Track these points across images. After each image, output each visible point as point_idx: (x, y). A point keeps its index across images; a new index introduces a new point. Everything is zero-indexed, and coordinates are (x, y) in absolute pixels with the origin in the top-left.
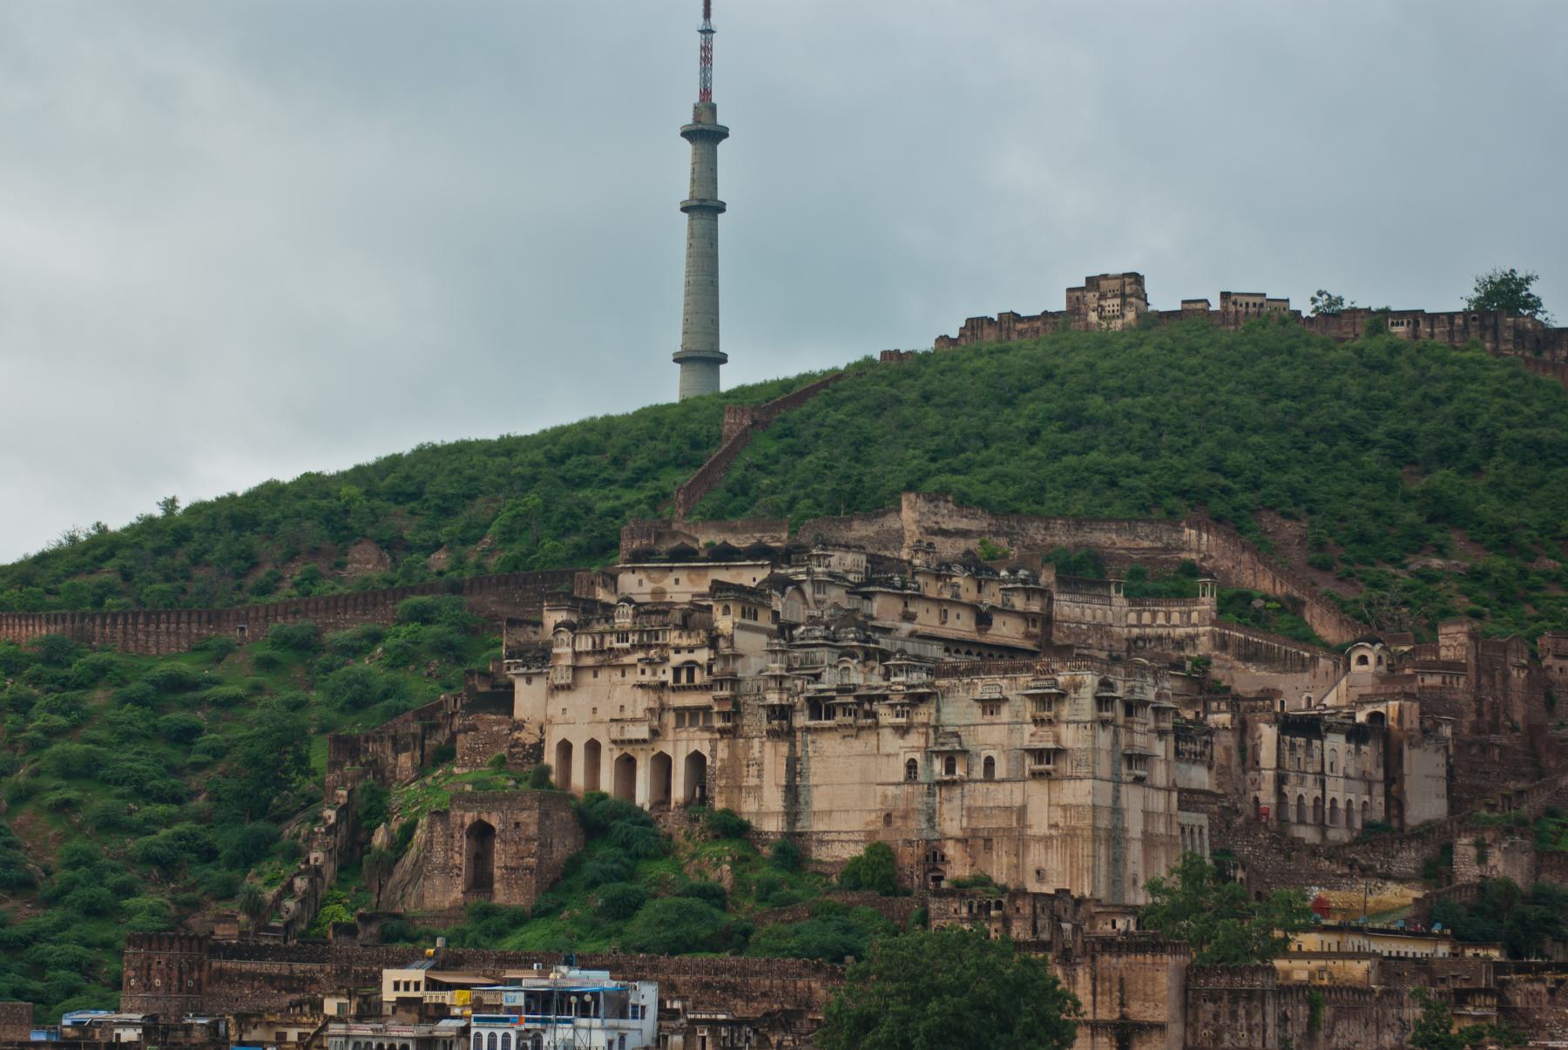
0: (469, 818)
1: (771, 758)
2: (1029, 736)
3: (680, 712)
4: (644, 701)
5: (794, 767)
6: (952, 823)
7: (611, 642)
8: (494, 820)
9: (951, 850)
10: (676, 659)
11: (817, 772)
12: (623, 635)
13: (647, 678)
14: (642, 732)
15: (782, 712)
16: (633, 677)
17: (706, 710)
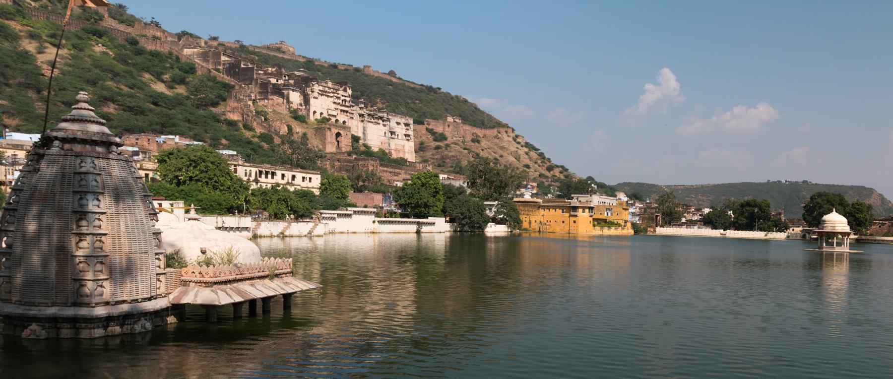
0: (336, 131)
1: (361, 125)
2: (404, 132)
3: (341, 110)
4: (333, 106)
5: (364, 128)
6: (393, 147)
7: (327, 89)
8: (342, 132)
9: (393, 152)
10: (343, 98)
11: (368, 131)
12: (329, 88)
13: (336, 101)
14: (334, 113)
15: (361, 115)
16: (332, 99)
17: (347, 112)
